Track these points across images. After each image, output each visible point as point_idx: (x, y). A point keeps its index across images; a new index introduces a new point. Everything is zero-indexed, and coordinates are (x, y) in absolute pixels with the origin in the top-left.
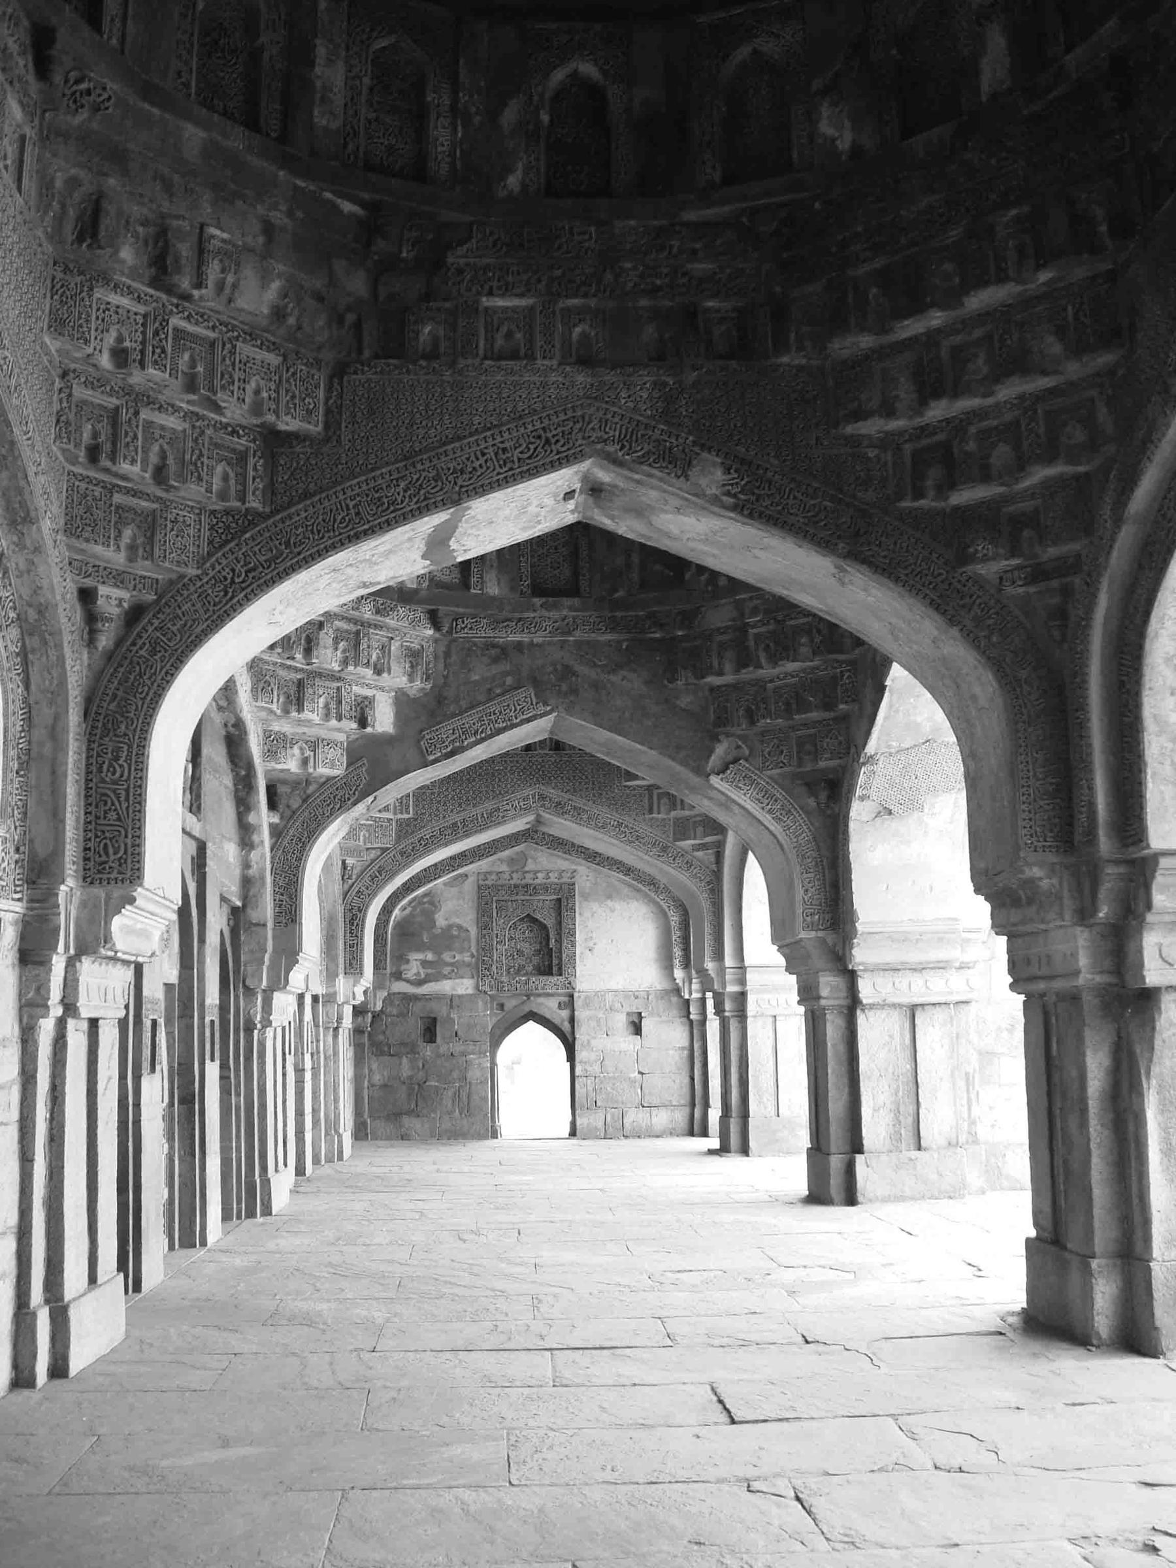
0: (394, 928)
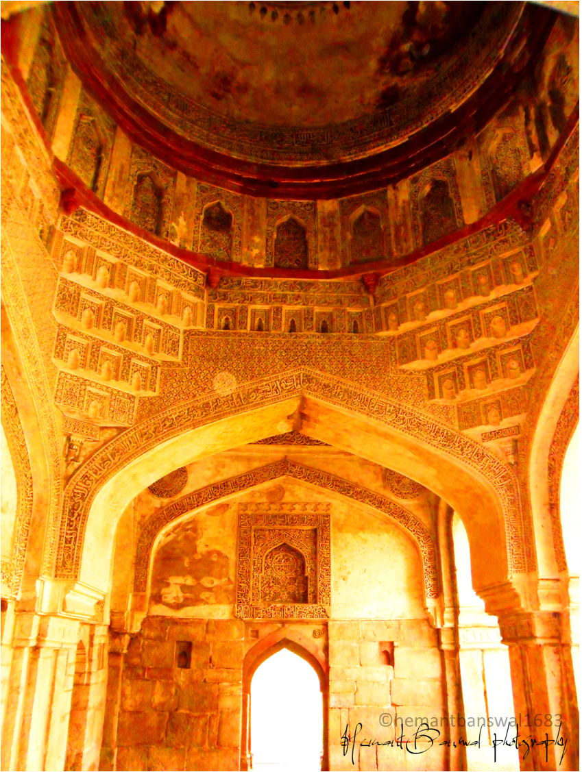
0: (158, 553)
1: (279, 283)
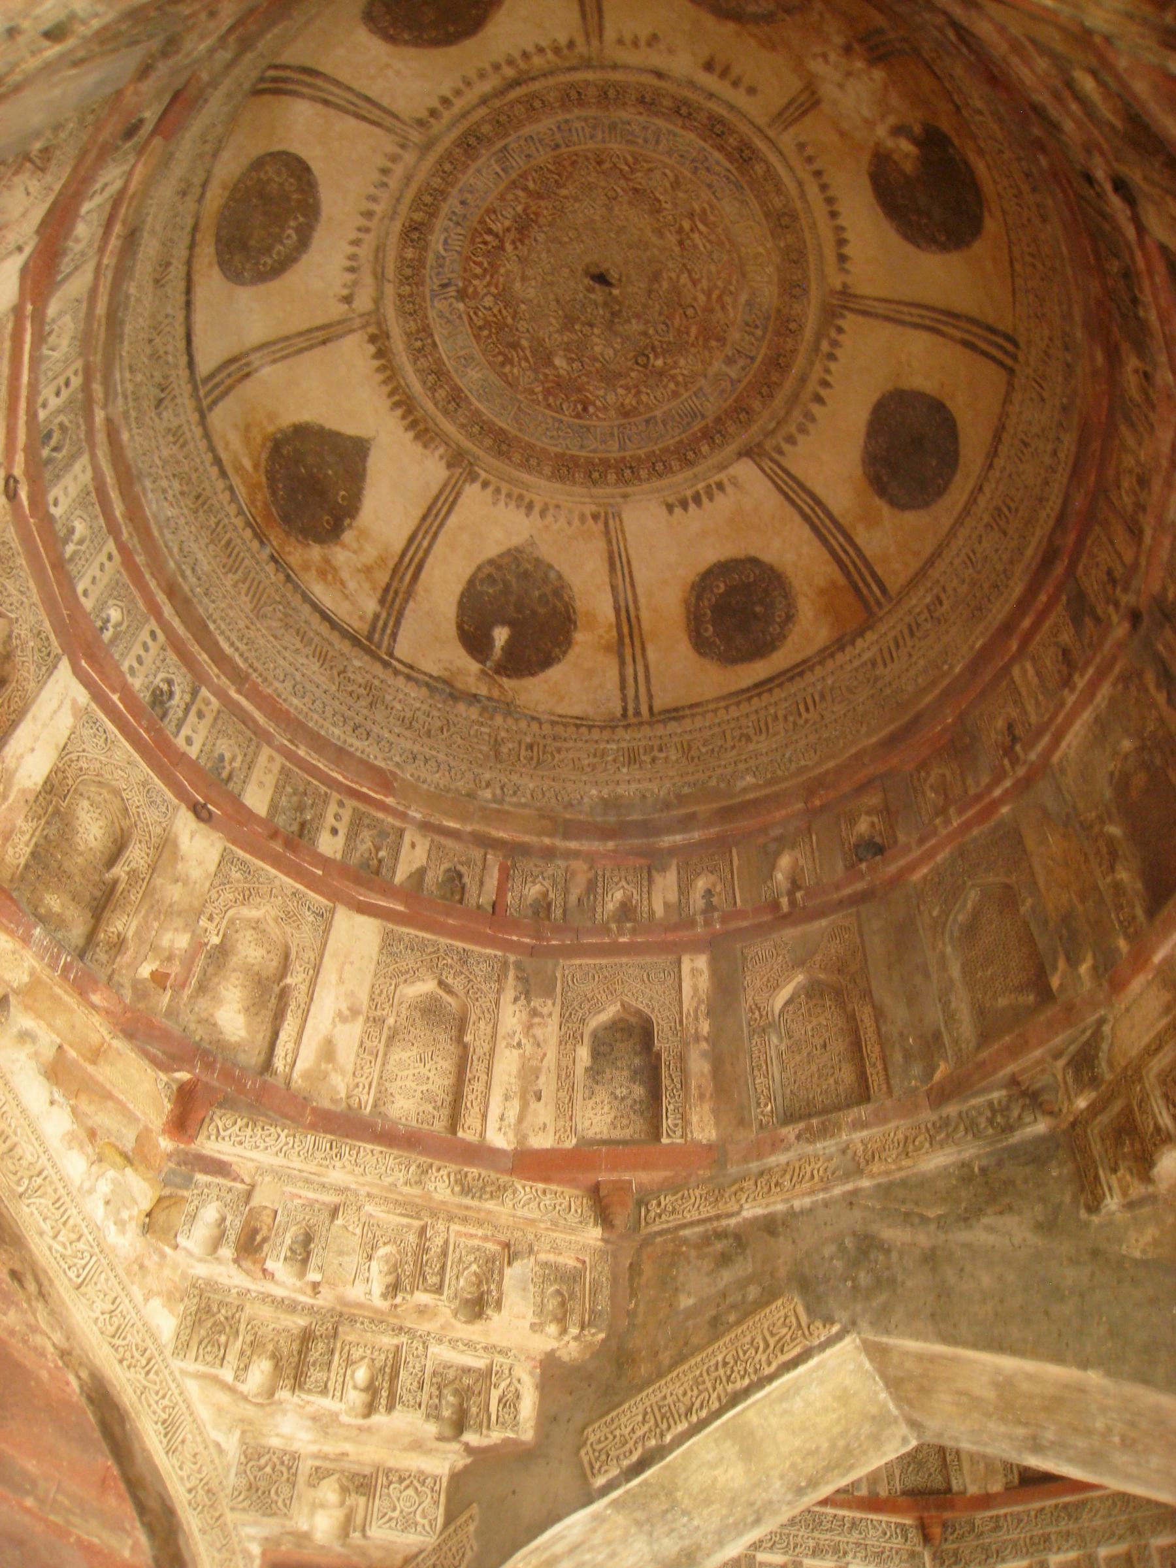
1: (1033, 1513)
